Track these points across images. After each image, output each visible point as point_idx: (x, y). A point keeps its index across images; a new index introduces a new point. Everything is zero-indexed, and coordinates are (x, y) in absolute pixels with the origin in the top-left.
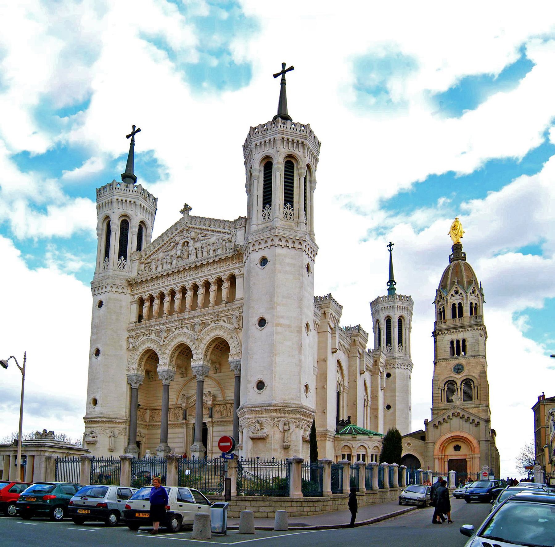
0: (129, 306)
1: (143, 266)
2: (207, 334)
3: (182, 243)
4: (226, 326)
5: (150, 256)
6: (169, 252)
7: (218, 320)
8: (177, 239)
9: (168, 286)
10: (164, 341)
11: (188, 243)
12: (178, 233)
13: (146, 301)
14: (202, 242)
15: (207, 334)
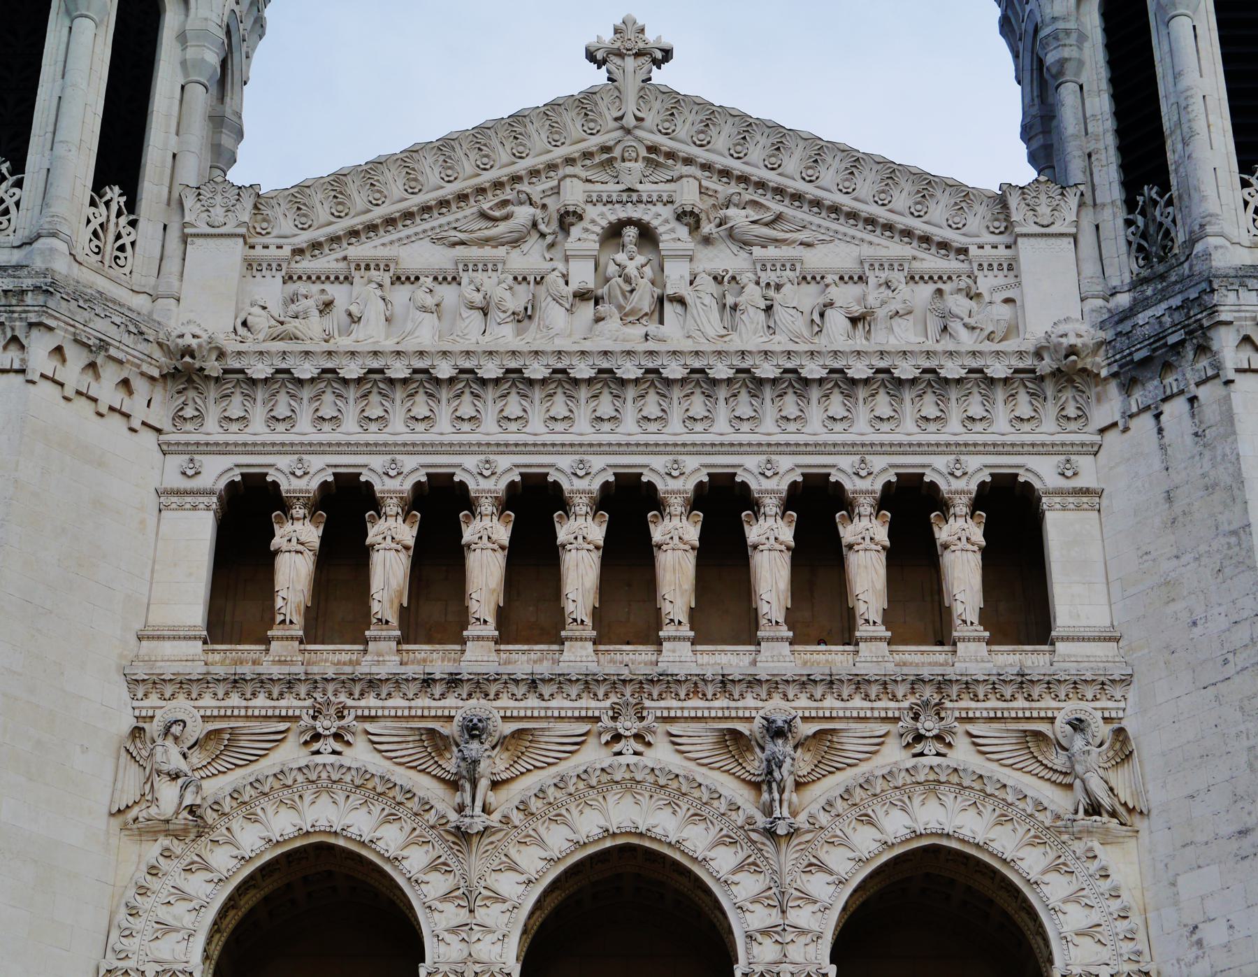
0: (152, 520)
1: (271, 289)
2: (855, 812)
3: (604, 223)
4: (1009, 783)
5: (335, 239)
6: (502, 251)
7: (939, 738)
8: (574, 194)
9: (504, 448)
10: (486, 809)
11: (647, 236)
12: (570, 161)
13: (298, 511)
14: (757, 251)
15: (855, 812)
